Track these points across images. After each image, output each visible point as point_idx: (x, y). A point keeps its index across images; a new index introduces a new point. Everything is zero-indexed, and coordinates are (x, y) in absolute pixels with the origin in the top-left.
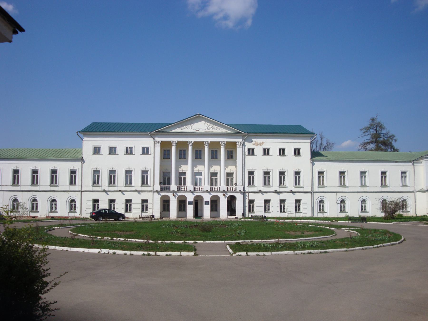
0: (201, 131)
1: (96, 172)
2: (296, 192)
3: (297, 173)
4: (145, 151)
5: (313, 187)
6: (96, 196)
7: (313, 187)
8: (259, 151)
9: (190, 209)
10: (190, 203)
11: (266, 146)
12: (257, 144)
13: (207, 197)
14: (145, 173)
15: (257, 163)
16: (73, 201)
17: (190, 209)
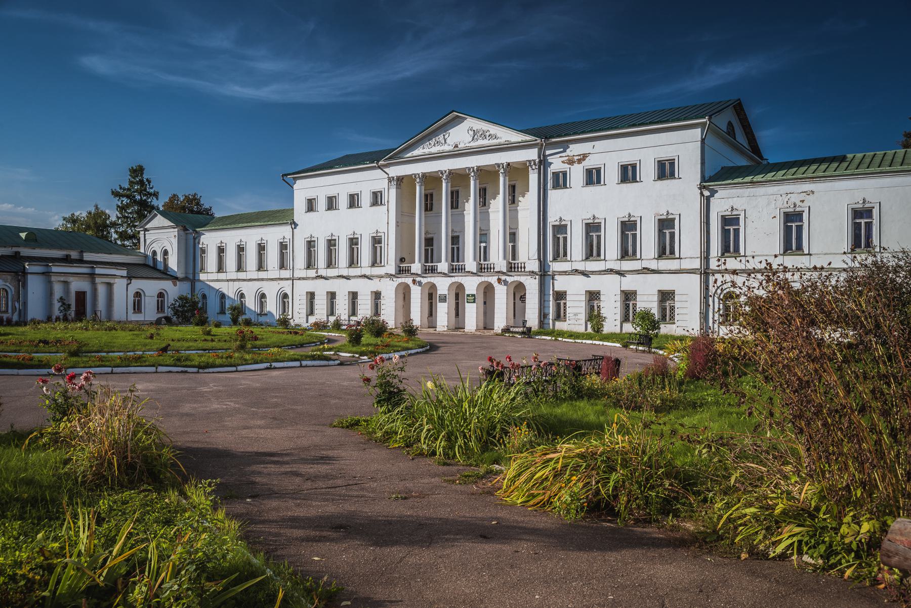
0: (461, 146)
1: (310, 245)
2: (593, 273)
3: (665, 224)
4: (377, 199)
5: (706, 258)
6: (310, 286)
7: (706, 258)
8: (577, 174)
9: (443, 312)
10: (443, 299)
11: (589, 163)
12: (571, 162)
13: (471, 285)
14: (376, 241)
15: (571, 205)
16: (263, 296)
17: (443, 312)
